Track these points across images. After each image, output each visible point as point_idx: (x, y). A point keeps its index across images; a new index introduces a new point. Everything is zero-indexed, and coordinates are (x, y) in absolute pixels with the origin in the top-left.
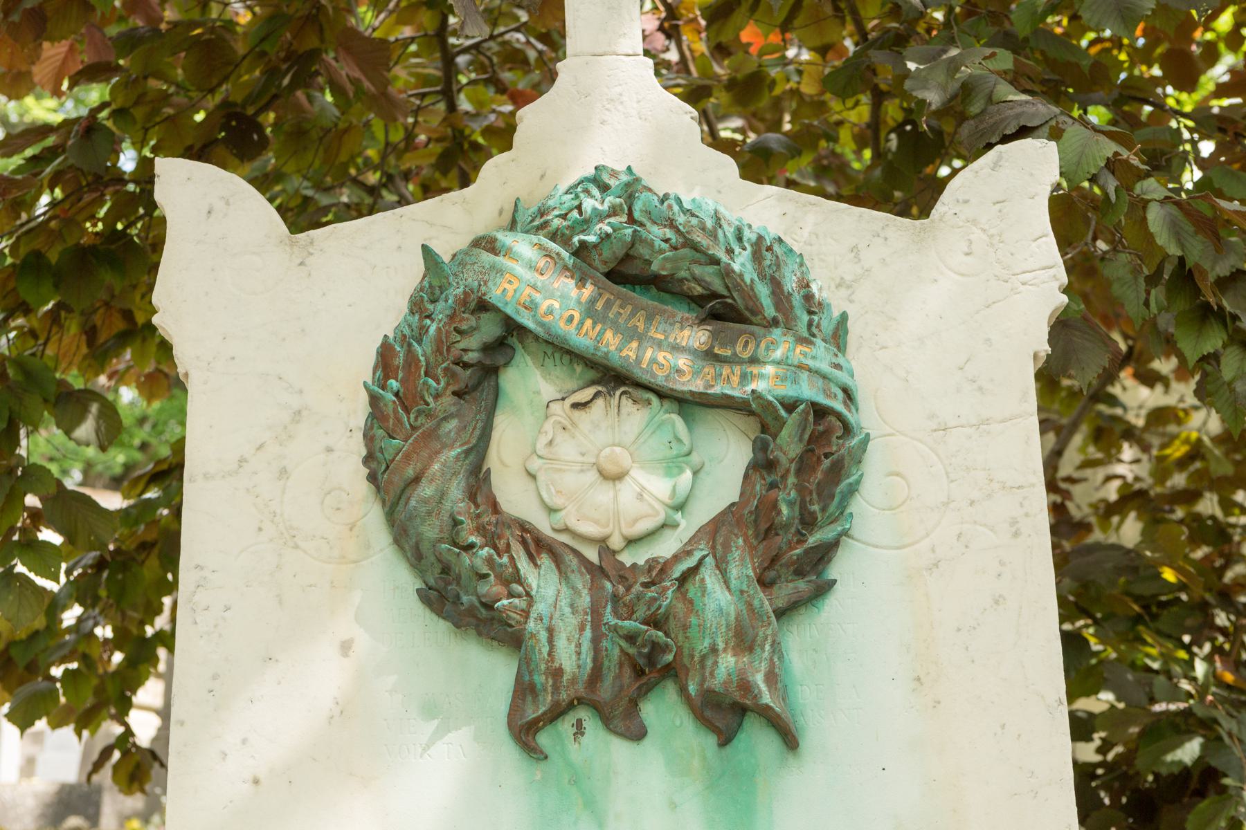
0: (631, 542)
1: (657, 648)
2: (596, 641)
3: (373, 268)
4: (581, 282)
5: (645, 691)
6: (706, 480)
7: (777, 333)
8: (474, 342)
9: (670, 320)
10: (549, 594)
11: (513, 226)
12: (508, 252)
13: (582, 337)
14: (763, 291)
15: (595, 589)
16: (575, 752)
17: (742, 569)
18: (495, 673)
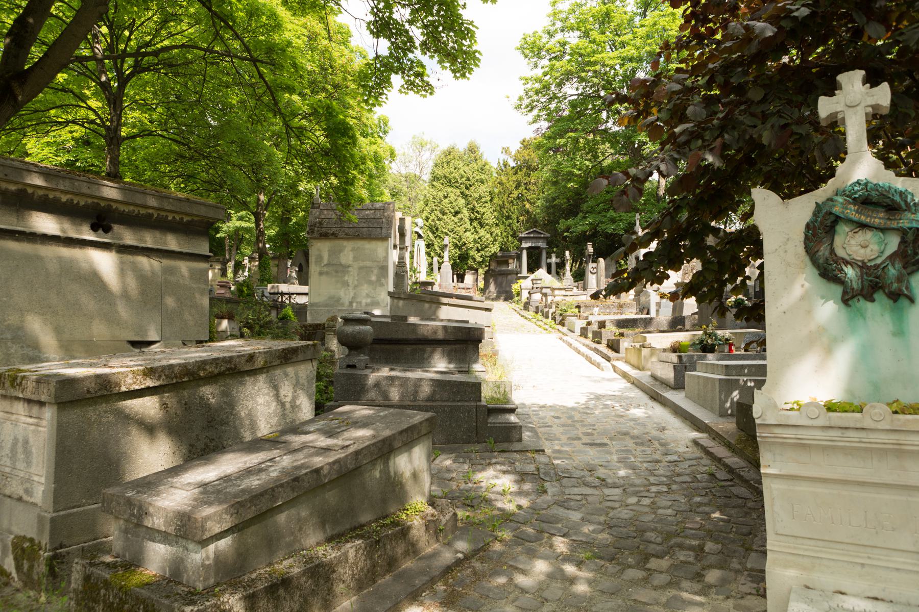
0: (869, 261)
1: (877, 283)
2: (862, 282)
3: (802, 208)
4: (855, 205)
5: (874, 292)
6: (888, 247)
7: (906, 213)
8: (829, 221)
9: (878, 212)
10: (850, 272)
11: (837, 195)
12: (836, 201)
13: (855, 216)
14: (902, 204)
15: (861, 271)
16: (858, 305)
17: (898, 265)
18: (838, 290)
